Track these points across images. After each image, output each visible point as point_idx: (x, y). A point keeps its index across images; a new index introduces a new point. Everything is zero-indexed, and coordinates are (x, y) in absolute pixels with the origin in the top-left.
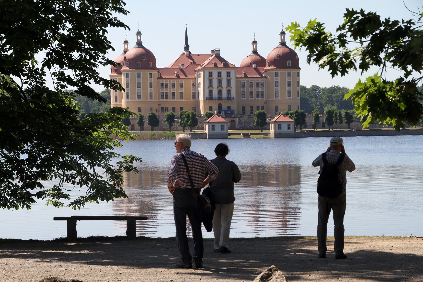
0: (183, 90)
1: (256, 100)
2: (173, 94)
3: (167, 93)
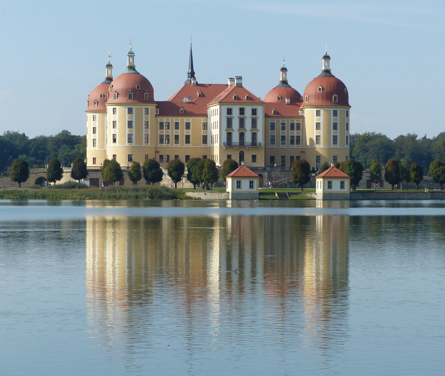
1: (290, 147)
2: (177, 137)
3: (168, 136)
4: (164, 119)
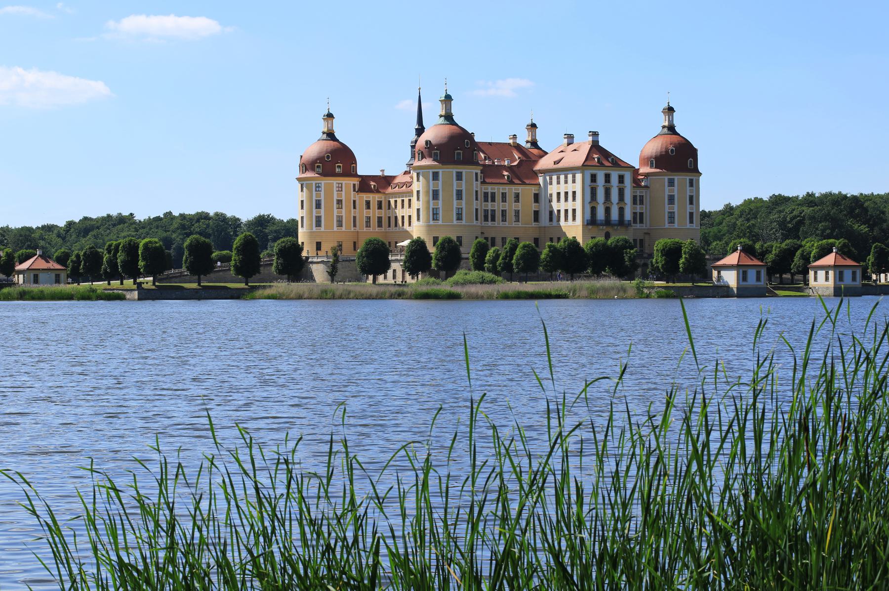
0: (520, 206)
2: (504, 213)
3: (493, 211)
4: (490, 189)
